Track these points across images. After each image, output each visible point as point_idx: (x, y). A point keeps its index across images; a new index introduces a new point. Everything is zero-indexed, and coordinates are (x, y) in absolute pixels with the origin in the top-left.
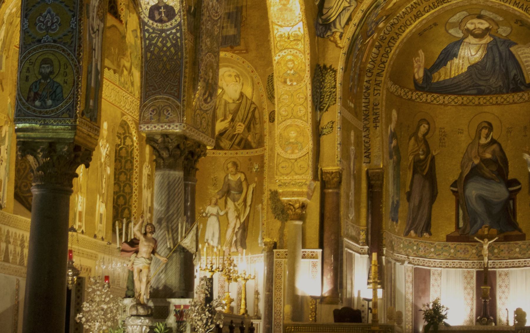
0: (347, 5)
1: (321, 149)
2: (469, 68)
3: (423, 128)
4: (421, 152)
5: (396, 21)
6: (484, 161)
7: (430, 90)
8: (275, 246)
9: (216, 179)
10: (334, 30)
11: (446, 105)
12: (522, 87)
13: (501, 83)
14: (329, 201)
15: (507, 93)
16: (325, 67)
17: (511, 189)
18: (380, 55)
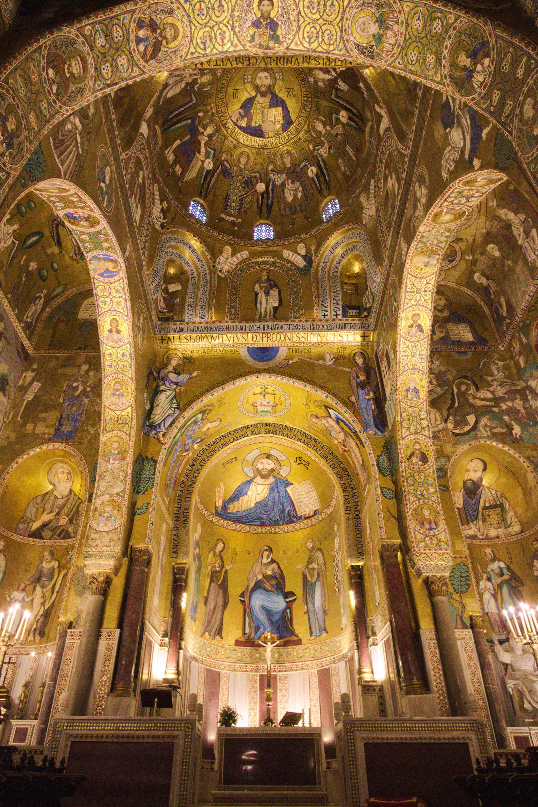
0: (172, 412)
1: (134, 527)
2: (255, 504)
3: (220, 546)
4: (217, 565)
5: (207, 448)
6: (266, 577)
7: (227, 518)
8: (71, 625)
9: (30, 564)
10: (159, 430)
11: (238, 531)
12: (295, 520)
13: (278, 518)
14: (135, 578)
15: (283, 524)
16: (147, 458)
17: (288, 600)
18: (193, 472)
